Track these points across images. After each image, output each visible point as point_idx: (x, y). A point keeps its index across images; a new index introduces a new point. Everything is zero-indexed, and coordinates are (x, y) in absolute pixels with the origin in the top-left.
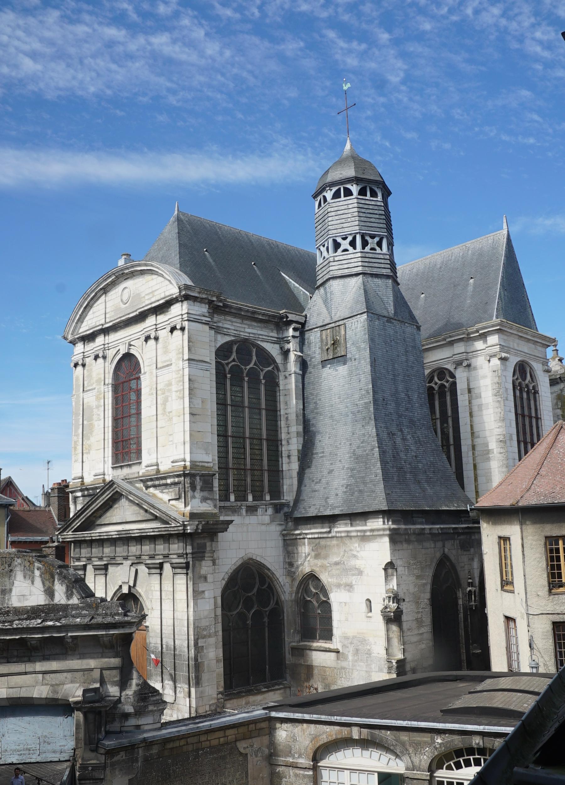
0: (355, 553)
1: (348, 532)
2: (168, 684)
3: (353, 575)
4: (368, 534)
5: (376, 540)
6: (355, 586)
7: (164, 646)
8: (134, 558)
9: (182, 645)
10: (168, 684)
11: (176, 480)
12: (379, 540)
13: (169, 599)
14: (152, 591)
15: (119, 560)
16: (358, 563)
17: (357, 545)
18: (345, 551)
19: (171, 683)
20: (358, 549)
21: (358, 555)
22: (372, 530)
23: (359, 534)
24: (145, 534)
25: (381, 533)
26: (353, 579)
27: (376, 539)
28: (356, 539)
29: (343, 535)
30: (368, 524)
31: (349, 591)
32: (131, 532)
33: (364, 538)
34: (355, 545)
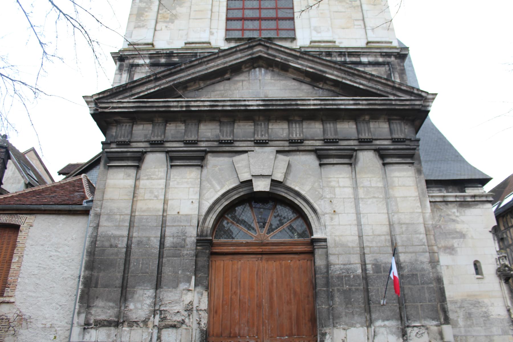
0: (454, 218)
1: (444, 196)
2: (385, 326)
3: (454, 238)
4: (469, 199)
5: (478, 206)
6: (458, 249)
7: (369, 267)
8: (287, 143)
9: (416, 260)
10: (385, 326)
11: (381, 60)
12: (481, 206)
13: (374, 197)
14: (334, 187)
15: (240, 146)
16: (459, 227)
17: (455, 210)
18: (440, 216)
19: (393, 324)
20: (457, 214)
21: (458, 219)
22: (474, 196)
23: (458, 200)
24: (335, 107)
25: (484, 199)
26: (455, 243)
27: (477, 205)
28: (454, 204)
29: (438, 199)
30: (467, 191)
31: (451, 254)
32: (299, 102)
33: (464, 204)
34: (453, 211)
